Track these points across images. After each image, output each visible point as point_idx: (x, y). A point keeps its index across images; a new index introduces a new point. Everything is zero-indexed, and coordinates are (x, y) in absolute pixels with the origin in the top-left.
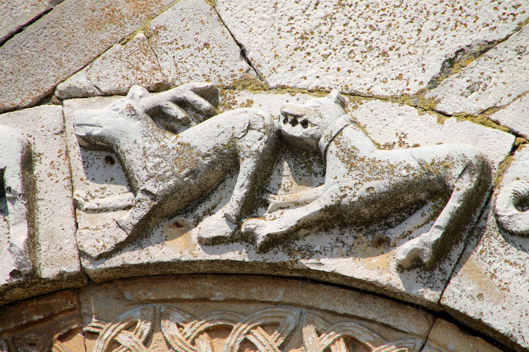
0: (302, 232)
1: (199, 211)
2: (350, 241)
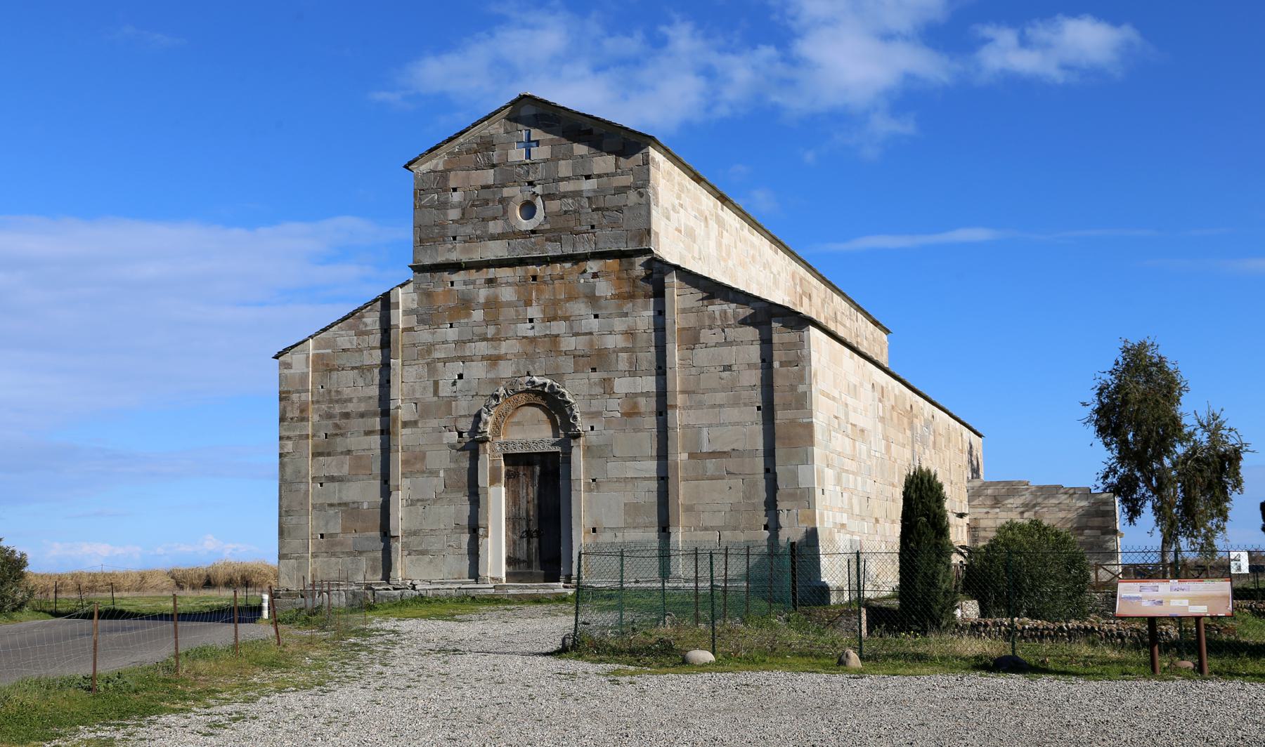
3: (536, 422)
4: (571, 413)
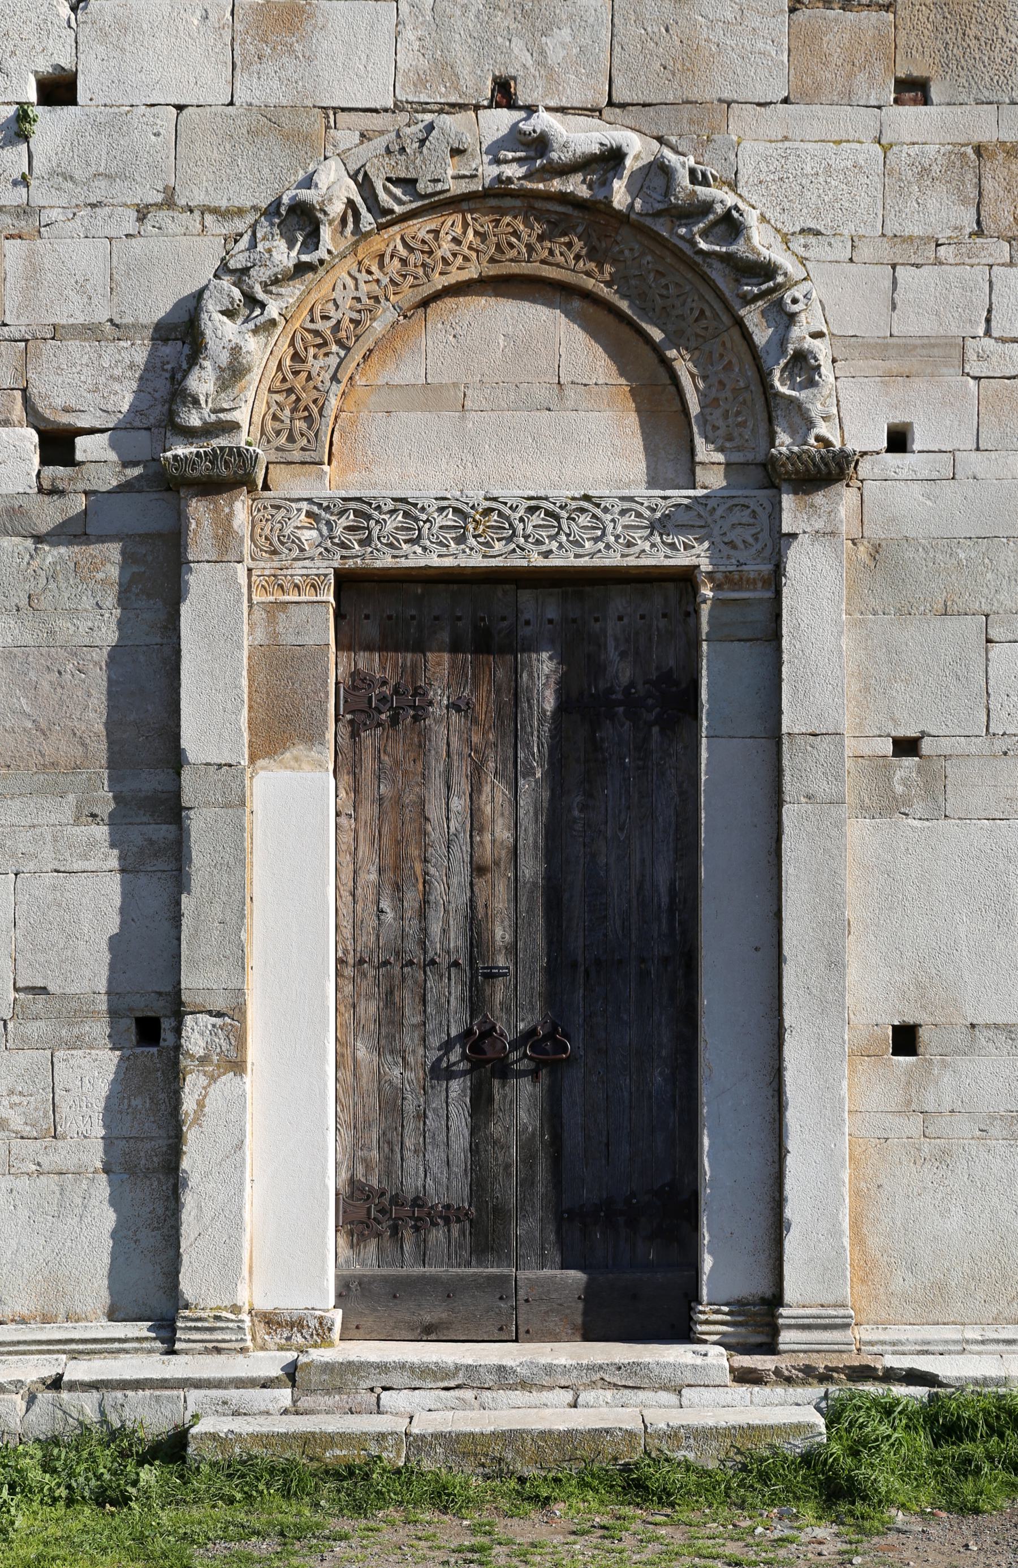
1: (683, 222)
3: (543, 394)
4: (783, 342)
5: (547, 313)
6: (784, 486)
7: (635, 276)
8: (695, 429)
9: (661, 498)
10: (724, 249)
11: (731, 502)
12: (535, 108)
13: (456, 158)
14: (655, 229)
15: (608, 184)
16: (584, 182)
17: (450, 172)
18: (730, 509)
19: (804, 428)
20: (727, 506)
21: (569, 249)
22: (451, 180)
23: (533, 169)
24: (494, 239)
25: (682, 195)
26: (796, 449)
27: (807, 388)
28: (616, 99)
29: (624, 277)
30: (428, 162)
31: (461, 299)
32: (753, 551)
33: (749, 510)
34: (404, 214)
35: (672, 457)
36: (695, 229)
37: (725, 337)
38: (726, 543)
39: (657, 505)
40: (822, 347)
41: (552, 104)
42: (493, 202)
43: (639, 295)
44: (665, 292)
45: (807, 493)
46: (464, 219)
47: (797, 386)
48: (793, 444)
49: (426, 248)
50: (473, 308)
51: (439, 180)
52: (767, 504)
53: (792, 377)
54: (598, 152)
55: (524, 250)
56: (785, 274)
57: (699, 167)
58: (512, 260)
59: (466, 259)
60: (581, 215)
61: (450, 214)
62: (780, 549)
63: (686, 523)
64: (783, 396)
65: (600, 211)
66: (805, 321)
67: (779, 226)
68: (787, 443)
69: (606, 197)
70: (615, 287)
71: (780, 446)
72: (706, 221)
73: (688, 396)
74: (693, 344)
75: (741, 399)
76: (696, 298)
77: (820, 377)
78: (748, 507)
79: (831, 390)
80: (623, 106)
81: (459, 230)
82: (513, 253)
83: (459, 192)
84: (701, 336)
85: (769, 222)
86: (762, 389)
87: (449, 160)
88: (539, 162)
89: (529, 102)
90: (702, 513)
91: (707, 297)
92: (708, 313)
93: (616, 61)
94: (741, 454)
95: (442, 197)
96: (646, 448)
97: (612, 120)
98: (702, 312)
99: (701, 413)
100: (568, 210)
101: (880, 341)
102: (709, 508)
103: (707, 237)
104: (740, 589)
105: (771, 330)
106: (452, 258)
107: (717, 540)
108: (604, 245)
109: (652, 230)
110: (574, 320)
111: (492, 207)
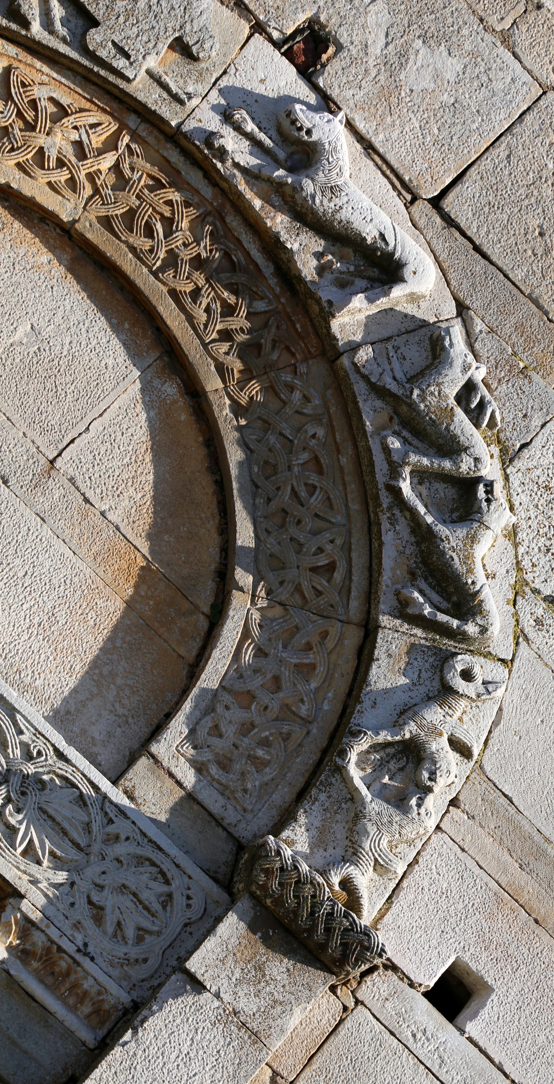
0: (407, 514)
1: (405, 433)
2: (408, 552)
5: (120, 360)
6: (244, 903)
7: (281, 434)
8: (187, 706)
9: (56, 750)
10: (429, 519)
11: (148, 852)
12: (333, 107)
13: (175, 56)
14: (361, 404)
15: (348, 290)
16: (319, 256)
17: (152, 62)
18: (140, 860)
19: (339, 852)
20: (139, 851)
21: (223, 315)
22: (143, 72)
23: (265, 172)
24: (134, 202)
25: (432, 400)
26: (304, 868)
27: (388, 802)
28: (448, 204)
29: (265, 422)
30: (132, 20)
31: (17, 225)
32: (120, 950)
33: (164, 889)
34: (39, 43)
35: (121, 711)
36: (413, 458)
37: (335, 629)
38: (90, 902)
39: (39, 753)
40: (454, 770)
41: (361, 126)
42: (175, 157)
43: (266, 462)
44: (303, 494)
45: (267, 942)
46: (116, 136)
47: (376, 786)
48: (306, 858)
49: (29, 115)
50: (22, 252)
51: (128, 56)
52: (198, 903)
53: (379, 767)
54: (369, 241)
55: (162, 255)
56: (484, 630)
57: (483, 390)
58: (133, 249)
59: (72, 183)
60: (278, 290)
61: (104, 111)
62: (161, 985)
63: (59, 819)
64: (347, 781)
65: (306, 311)
66: (458, 714)
67: (526, 563)
68: (299, 848)
69: (330, 303)
70: (243, 422)
71: (285, 841)
72: (436, 462)
73: (216, 654)
74: (284, 594)
75: (286, 729)
76: (339, 542)
77: (419, 806)
78: (167, 882)
79: (419, 836)
80: (450, 222)
81: (97, 140)
82: (144, 243)
83: (141, 97)
84: (304, 597)
85: (516, 545)
86: (325, 744)
87: (163, 47)
88: (280, 172)
89: (334, 93)
90: (95, 827)
91: (354, 555)
92: (338, 576)
93: (487, 163)
94: (222, 800)
95: (112, 78)
96: (95, 664)
97: (422, 223)
98: (331, 568)
99: (215, 693)
100: (267, 269)
101: (537, 837)
102: (111, 829)
103: (420, 483)
104: (52, 989)
105: (403, 681)
106: (53, 164)
107: (83, 885)
108: (275, 356)
109: (356, 403)
110: (148, 406)
111: (168, 161)
